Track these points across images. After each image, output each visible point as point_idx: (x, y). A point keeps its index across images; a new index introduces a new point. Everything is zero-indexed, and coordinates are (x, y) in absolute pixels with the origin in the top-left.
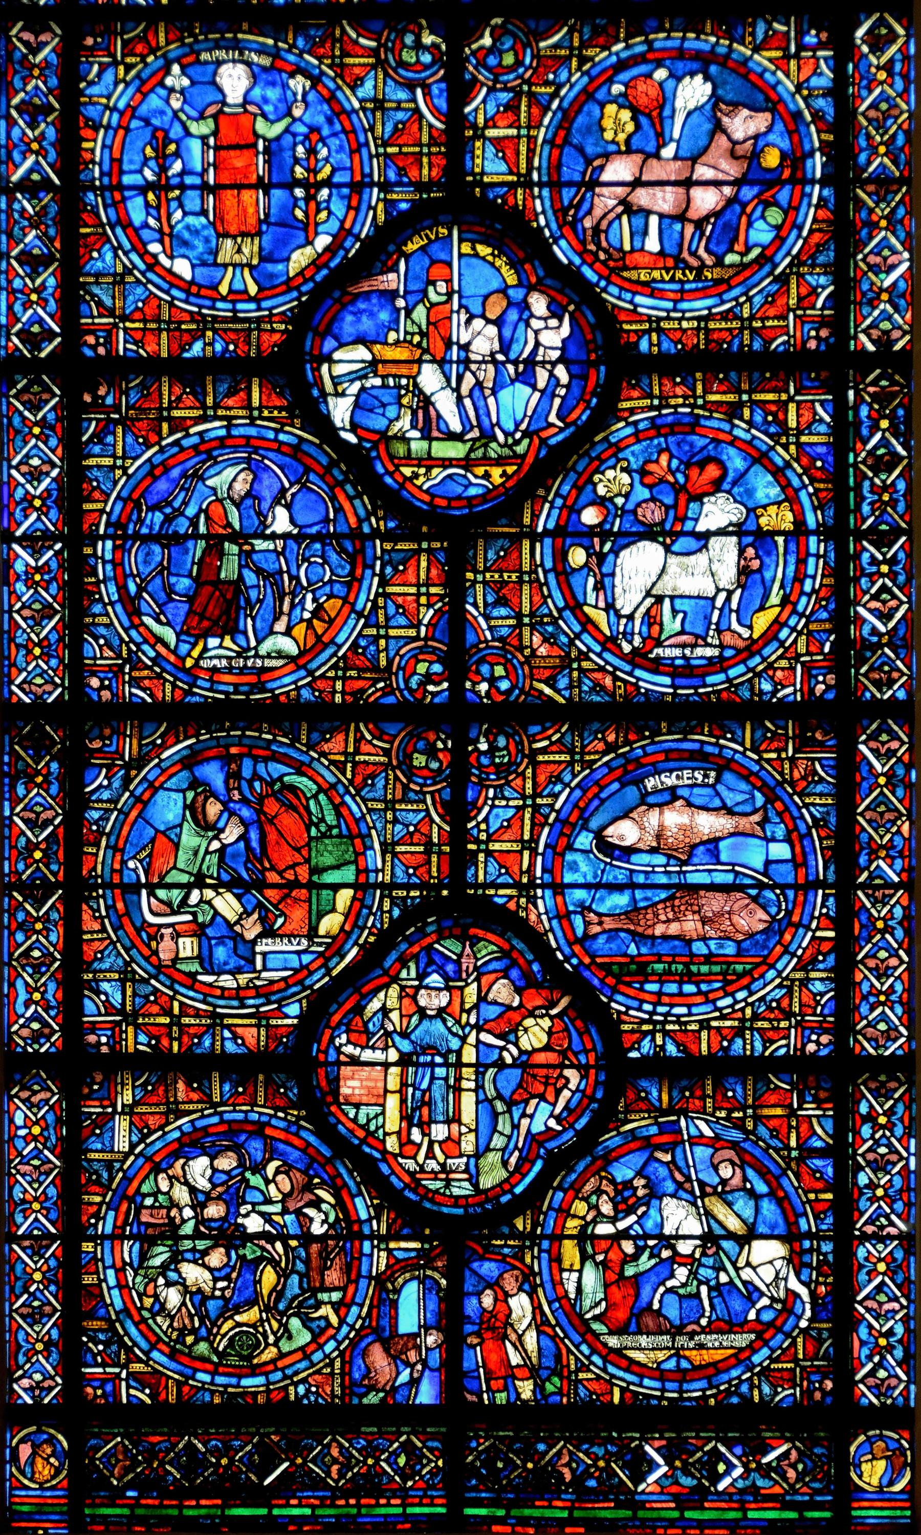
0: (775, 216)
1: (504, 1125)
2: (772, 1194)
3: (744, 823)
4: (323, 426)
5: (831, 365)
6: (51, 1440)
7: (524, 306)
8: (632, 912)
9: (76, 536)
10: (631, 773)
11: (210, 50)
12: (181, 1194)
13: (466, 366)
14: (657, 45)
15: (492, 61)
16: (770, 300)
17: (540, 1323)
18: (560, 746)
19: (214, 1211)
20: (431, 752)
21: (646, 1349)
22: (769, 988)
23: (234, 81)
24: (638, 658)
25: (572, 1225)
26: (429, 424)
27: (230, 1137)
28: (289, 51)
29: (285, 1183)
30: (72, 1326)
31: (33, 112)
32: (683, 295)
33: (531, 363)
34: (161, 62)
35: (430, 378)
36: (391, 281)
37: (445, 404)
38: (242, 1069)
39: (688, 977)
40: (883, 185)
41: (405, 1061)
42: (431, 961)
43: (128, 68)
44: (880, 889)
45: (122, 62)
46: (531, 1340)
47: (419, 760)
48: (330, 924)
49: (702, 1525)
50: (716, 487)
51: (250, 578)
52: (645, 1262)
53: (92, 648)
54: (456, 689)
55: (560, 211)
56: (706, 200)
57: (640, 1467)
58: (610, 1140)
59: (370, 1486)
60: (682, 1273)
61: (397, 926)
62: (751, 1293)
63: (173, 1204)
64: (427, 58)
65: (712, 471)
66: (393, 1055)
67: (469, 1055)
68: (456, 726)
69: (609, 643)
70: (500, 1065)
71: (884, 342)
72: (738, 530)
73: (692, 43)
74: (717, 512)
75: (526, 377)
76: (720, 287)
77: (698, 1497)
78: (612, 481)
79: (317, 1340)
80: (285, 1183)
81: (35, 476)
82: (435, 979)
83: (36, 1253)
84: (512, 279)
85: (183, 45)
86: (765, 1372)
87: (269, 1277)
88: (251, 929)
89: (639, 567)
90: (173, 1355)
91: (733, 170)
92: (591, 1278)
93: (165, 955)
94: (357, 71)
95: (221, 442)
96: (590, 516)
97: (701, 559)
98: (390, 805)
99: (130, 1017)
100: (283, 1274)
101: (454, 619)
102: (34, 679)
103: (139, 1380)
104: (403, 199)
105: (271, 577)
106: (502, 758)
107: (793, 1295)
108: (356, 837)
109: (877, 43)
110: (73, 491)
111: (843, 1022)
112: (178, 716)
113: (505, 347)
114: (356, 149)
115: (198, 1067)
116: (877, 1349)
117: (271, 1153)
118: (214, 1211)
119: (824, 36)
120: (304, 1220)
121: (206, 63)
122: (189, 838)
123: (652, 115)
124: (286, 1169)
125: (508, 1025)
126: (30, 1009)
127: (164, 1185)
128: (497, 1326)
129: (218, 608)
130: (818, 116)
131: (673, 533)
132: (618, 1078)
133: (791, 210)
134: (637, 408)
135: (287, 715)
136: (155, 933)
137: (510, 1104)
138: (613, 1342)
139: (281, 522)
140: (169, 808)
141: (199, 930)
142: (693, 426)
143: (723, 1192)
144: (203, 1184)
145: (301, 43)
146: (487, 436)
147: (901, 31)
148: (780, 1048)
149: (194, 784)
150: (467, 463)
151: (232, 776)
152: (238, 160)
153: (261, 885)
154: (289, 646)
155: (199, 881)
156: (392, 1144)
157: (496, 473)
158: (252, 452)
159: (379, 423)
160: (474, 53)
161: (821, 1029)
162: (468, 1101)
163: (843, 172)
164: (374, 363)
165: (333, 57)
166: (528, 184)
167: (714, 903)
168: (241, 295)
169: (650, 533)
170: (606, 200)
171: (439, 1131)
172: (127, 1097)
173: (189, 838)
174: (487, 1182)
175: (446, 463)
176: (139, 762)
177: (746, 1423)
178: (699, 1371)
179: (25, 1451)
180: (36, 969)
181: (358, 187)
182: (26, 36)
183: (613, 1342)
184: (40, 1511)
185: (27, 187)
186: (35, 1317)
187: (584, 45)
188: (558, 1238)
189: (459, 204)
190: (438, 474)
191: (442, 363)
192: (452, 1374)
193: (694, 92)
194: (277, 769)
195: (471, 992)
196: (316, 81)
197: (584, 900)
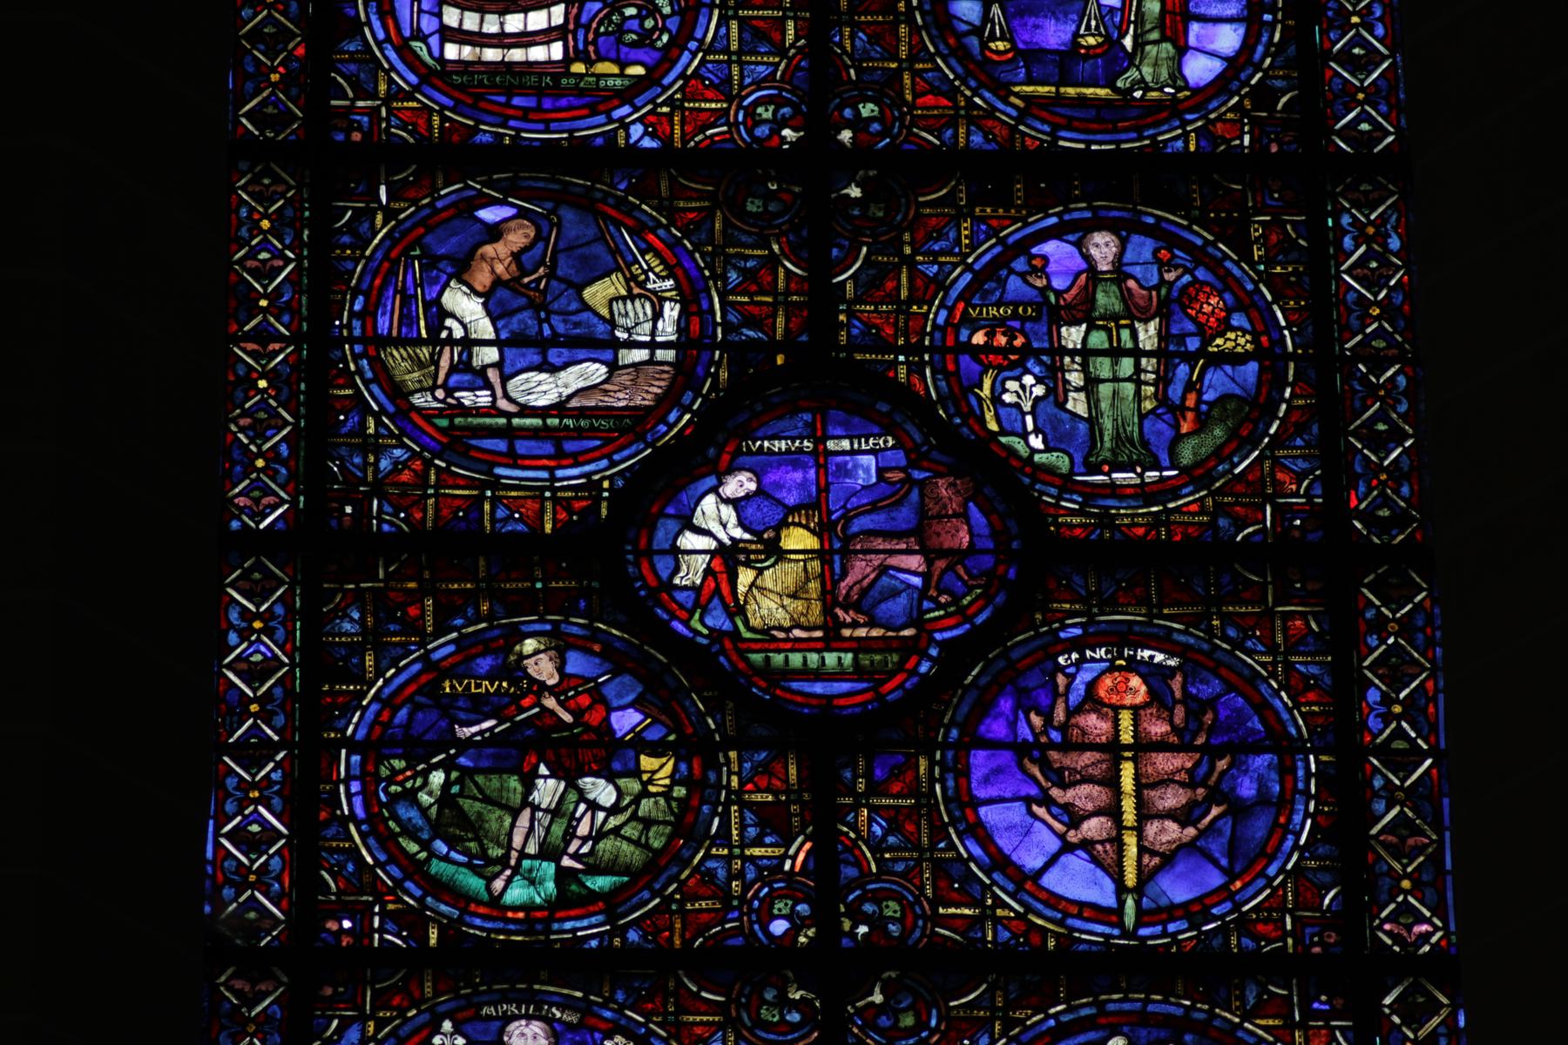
11: (495, 1004)
14: (1111, 1007)
15: (884, 1021)
28: (604, 1006)
34: (426, 1017)
43: (380, 1025)
45: (372, 1017)
64: (795, 1017)
85: (458, 997)
94: (698, 1031)
119: (1339, 1002)
121: (489, 1018)
145: (620, 996)
147: (1445, 1001)
160: (859, 1012)
165: (666, 1013)
182: (238, 984)
187: (1010, 1005)
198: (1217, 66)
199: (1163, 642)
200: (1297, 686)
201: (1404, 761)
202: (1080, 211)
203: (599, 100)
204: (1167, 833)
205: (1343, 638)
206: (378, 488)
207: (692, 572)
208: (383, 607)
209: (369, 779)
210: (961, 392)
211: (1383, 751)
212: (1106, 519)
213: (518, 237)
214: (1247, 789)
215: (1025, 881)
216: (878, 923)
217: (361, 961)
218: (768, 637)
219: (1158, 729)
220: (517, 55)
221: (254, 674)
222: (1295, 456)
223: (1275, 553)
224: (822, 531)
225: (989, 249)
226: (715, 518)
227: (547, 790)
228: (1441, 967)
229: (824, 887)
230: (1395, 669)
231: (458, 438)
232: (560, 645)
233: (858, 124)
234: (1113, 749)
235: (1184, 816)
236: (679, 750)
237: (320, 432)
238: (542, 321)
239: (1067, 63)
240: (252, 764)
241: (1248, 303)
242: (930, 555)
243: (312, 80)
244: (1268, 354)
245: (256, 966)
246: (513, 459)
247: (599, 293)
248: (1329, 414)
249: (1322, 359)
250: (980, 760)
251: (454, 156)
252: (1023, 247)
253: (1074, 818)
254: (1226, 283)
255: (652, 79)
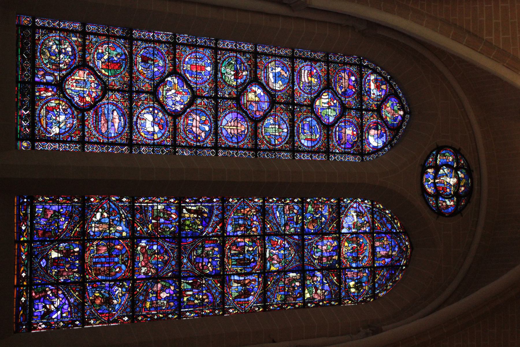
0: (192, 138)
1: (75, 94)
2: (65, 131)
3: (116, 130)
4: (167, 77)
5: (175, 145)
6: (30, 23)
7: (182, 104)
8: (104, 114)
9: (154, 42)
10: (123, 115)
12: (66, 46)
13: (175, 96)
16: (182, 137)
17: (47, 97)
18: (127, 105)
19: (63, 51)
20: (126, 87)
21: (43, 112)
22: (94, 133)
23: (209, 69)
24: (138, 117)
25: (61, 102)
26: (168, 90)
27: (74, 54)
29: (67, 61)
30: (47, 28)
31: (205, 42)
32: (183, 126)
33: (175, 105)
35: (173, 91)
36: (185, 87)
37: (170, 93)
38: (83, 57)
39: (95, 122)
40: (196, 153)
41: (84, 80)
42: (98, 85)
44: (107, 149)
46: (45, 95)
47: (125, 86)
48: (103, 71)
49: (17, 119)
50: (160, 129)
51: (149, 65)
52: (56, 113)
53: (140, 42)
54: (134, 92)
55: (193, 110)
56: (194, 129)
57: (26, 110)
58: (73, 109)
59: (23, 70)
60: (54, 118)
61: (103, 81)
62: (51, 128)
63: (64, 45)
65: (162, 128)
66: (85, 79)
67: (85, 89)
68: (130, 91)
69: (140, 113)
70: (84, 94)
71: (177, 152)
72: (154, 131)
73: (213, 129)
74: (157, 129)
75: (173, 104)
76: (184, 130)
77: (21, 118)
78: (160, 115)
79: (44, 64)
80: (67, 61)
81: (162, 37)
82: (96, 85)
83: (58, 24)
84: (185, 103)
86: (40, 129)
87: (54, 58)
88: (103, 60)
89: (149, 117)
90: (43, 43)
91: (198, 133)
92: (53, 105)
93: (99, 48)
95: (166, 62)
96: (156, 111)
97: (151, 126)
98: (119, 81)
99: (91, 42)
100: (54, 60)
101: (143, 92)
102: (136, 34)
103: (39, 37)
104: (195, 89)
105: (149, 68)
106: (125, 97)
107: (51, 134)
108: (115, 76)
109: (212, 152)
110: (160, 42)
111: (89, 143)
112: (131, 53)
113: (177, 102)
114: (201, 84)
115: (84, 51)
116: (43, 146)
117: (72, 60)
118: (63, 51)
120: (62, 64)
122: (115, 53)
123: (204, 123)
124: (69, 62)
125: (89, 95)
126: (91, 28)
127: (67, 44)
128: (47, 90)
129: (145, 60)
130: (204, 144)
131: (154, 123)
132: (82, 110)
133: (193, 140)
134: (169, 119)
135: (131, 68)
136: (102, 47)
137: (78, 95)
138: (44, 107)
139: (156, 69)
140: (119, 50)
141: (103, 53)
142: (167, 126)
143: (66, 125)
144: (67, 50)
146: (166, 98)
148: (86, 134)
149: (122, 54)
150: (163, 95)
151: (123, 60)
152: (199, 68)
153: (109, 62)
154: (140, 69)
155: (109, 54)
156: (73, 77)
157: (161, 99)
158: (165, 66)
159: (168, 84)
161: (89, 139)
162: (79, 89)
163: (198, 147)
164: (175, 84)
166: (196, 106)
167: (106, 125)
168: (184, 67)
169: (154, 119)
170: (194, 116)
171: (75, 84)
172: (80, 40)
173: (115, 53)
174: (67, 90)
175: (163, 92)
176: (125, 47)
177: (32, 126)
178: (40, 119)
179: (28, 19)
180: (97, 29)
181: (196, 84)
183: (44, 107)
184: (19, 21)
185: (196, 40)
186: (48, 23)
188: (59, 100)
189: (194, 97)
190: (161, 91)
191: (175, 93)
192: (40, 83)
193: (207, 128)
194: (124, 66)
195: (94, 90)
196: (209, 79)
197: (106, 107)
198: (303, 143)
199: (247, 132)
200: (243, 145)
201: (236, 154)
202: (289, 129)
203: (299, 84)
204: (229, 131)
205: (248, 149)
206: (261, 60)
207: (253, 88)
208: (250, 59)
209: (233, 56)
210: (271, 116)
211: (237, 152)
212: (259, 128)
213: (286, 75)
214: (233, 139)
215: (225, 117)
216: (220, 103)
217: (216, 54)
218: (247, 95)
219: (239, 131)
220: (303, 77)
221: (243, 47)
222: (266, 147)
223: (256, 144)
224: (258, 101)
225: (285, 120)
226: (259, 91)
227: (233, 73)
228: (217, 155)
229: (223, 98)
230: (245, 154)
231: (266, 68)
232: (247, 75)
233: (297, 108)
234: (237, 127)
235: (231, 133)
236: (236, 86)
237: (266, 54)
238: (277, 77)
239: (303, 129)
240: (235, 46)
241: (280, 144)
242: (256, 111)
243: (300, 58)
244: (275, 145)
245: (216, 44)
246: (264, 73)
247: (280, 82)
248: (270, 150)
249: (275, 150)
250: (236, 114)
251: (293, 70)
252: (285, 123)
253: (230, 122)
254: (282, 142)
255: (301, 89)
